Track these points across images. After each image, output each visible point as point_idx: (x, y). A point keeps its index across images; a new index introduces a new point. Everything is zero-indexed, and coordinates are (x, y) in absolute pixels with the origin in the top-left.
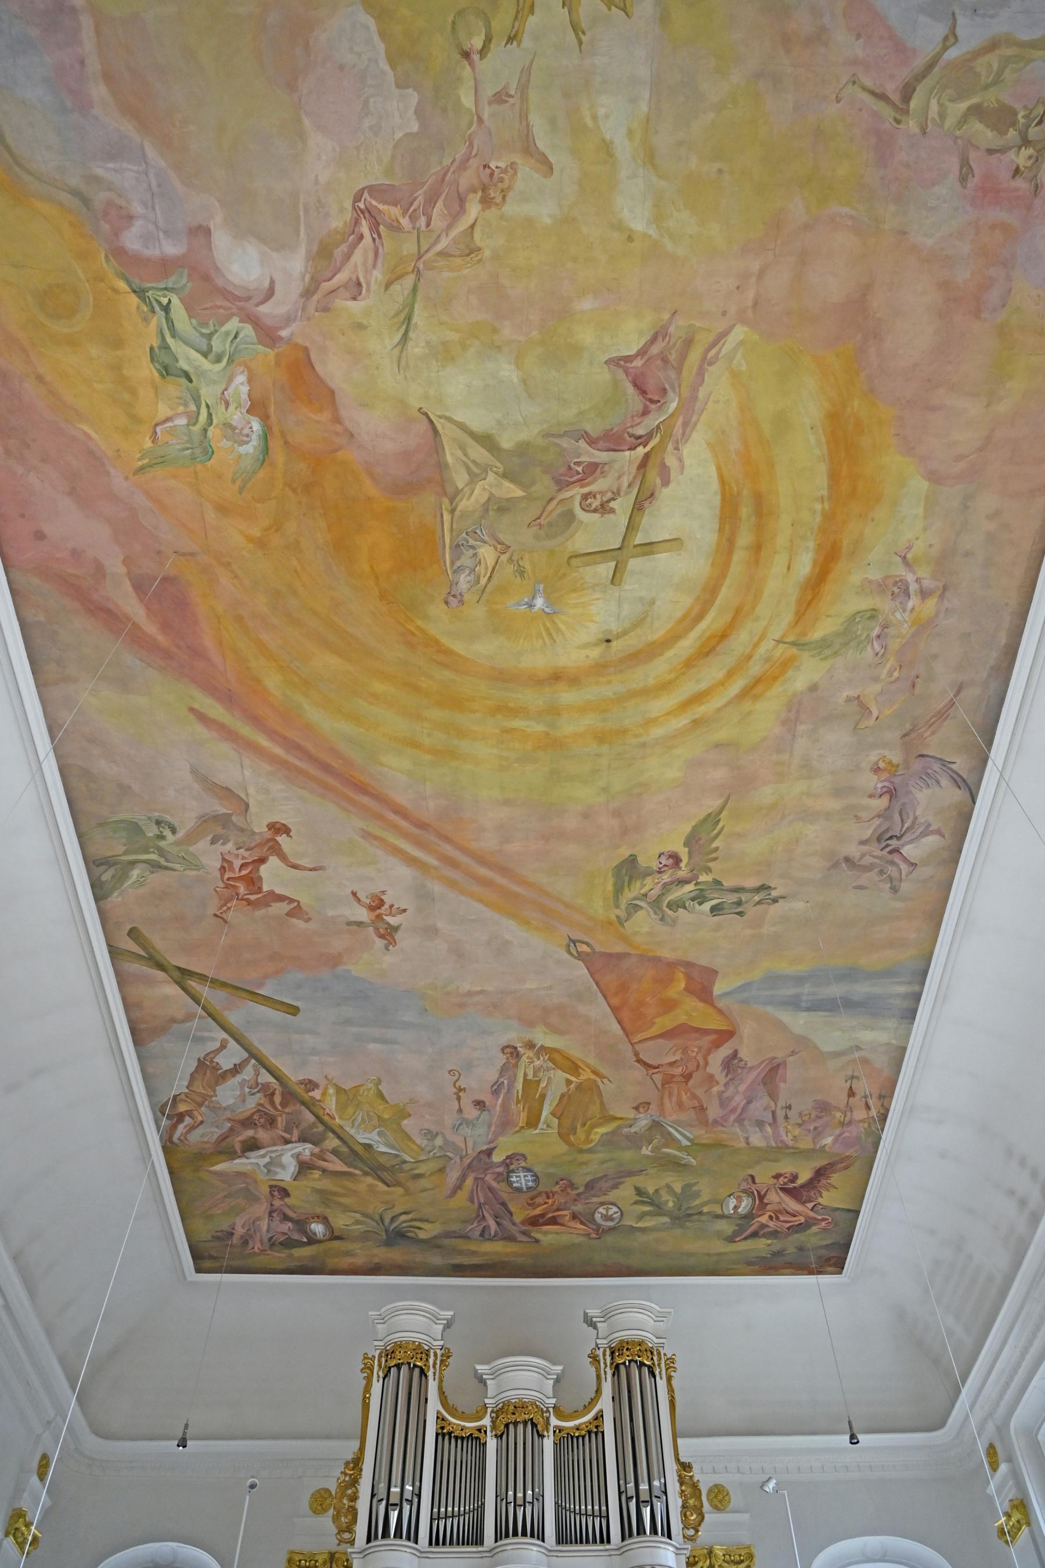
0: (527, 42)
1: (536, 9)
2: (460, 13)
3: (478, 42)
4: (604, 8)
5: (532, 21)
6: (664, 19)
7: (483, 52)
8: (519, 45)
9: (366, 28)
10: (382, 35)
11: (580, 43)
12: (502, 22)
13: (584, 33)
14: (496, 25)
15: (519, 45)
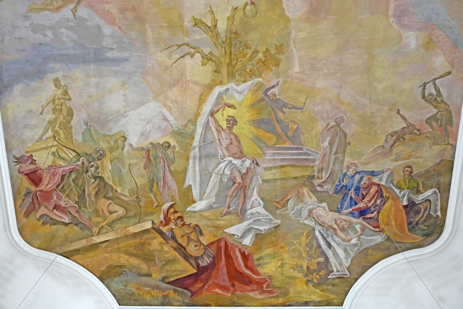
0: (230, 8)
1: (227, 18)
2: (254, 17)
3: (248, 7)
4: (202, 19)
5: (228, 14)
6: (180, 16)
7: (246, 4)
8: (233, 6)
9: (288, 11)
10: (283, 9)
11: (210, 8)
12: (239, 14)
13: (209, 11)
14: (241, 13)
15: (233, 6)
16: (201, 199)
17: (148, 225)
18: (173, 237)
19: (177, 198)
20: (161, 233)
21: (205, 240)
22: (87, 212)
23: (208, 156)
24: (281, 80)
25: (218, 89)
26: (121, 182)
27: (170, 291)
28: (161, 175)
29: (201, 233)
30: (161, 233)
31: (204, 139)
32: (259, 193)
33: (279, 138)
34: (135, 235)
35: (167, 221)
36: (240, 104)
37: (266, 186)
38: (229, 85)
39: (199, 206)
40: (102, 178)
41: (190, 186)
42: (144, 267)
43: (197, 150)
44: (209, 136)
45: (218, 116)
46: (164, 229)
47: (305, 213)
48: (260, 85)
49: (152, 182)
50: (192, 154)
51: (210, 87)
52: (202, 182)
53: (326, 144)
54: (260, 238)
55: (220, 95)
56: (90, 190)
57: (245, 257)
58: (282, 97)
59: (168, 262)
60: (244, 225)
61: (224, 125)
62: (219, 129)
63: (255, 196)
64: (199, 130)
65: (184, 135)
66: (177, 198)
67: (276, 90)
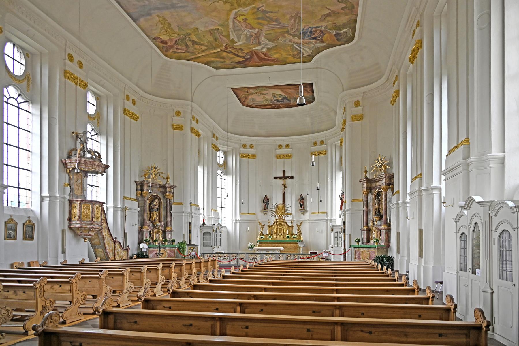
16: (239, 41)
17: (219, 50)
18: (231, 52)
19: (228, 42)
20: (225, 52)
21: (245, 52)
22: (191, 49)
23: (238, 30)
24: (264, 5)
25: (234, 11)
26: (201, 40)
27: (236, 65)
28: (219, 37)
29: (242, 50)
30: (225, 52)
31: (234, 26)
32: (265, 37)
33: (269, 21)
34: (214, 53)
35: (226, 48)
36: (247, 14)
37: (267, 36)
38: (240, 9)
39: (239, 43)
40: (193, 40)
41: (233, 39)
42: (222, 60)
43: (232, 29)
44: (236, 24)
45: (238, 18)
46: (227, 50)
47: (288, 41)
48: (254, 8)
49: (215, 39)
50: (230, 30)
51: (231, 10)
52: (238, 38)
53: (292, 21)
54: (269, 49)
55: (236, 13)
56: (189, 43)
57: (264, 54)
58: (267, 10)
59: (231, 58)
60: (261, 46)
61: (242, 21)
62: (239, 22)
63: (263, 38)
64: (230, 24)
65: (225, 25)
66: (228, 42)
67: (263, 8)
